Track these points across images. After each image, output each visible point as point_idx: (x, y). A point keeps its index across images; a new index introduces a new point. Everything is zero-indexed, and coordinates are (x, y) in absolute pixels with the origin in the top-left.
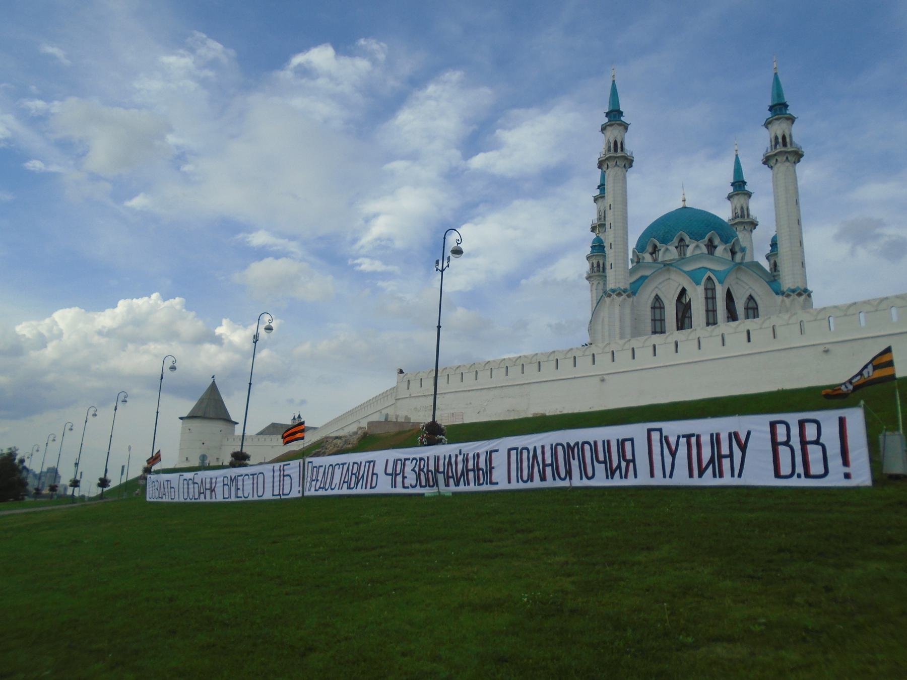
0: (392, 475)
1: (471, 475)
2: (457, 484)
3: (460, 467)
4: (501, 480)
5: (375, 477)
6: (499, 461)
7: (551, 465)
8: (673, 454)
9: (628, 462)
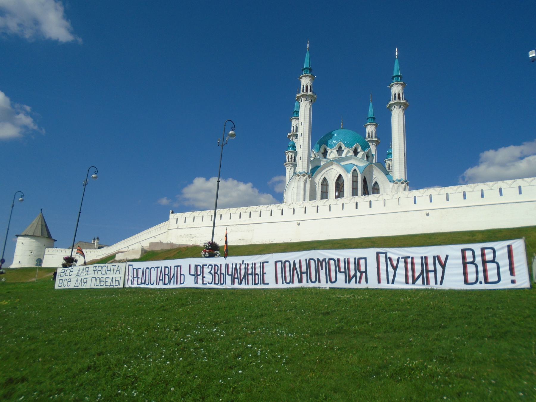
0: (194, 275)
1: (250, 277)
2: (240, 283)
3: (243, 272)
4: (271, 282)
5: (182, 277)
6: (269, 269)
7: (306, 273)
8: (395, 268)
9: (362, 273)
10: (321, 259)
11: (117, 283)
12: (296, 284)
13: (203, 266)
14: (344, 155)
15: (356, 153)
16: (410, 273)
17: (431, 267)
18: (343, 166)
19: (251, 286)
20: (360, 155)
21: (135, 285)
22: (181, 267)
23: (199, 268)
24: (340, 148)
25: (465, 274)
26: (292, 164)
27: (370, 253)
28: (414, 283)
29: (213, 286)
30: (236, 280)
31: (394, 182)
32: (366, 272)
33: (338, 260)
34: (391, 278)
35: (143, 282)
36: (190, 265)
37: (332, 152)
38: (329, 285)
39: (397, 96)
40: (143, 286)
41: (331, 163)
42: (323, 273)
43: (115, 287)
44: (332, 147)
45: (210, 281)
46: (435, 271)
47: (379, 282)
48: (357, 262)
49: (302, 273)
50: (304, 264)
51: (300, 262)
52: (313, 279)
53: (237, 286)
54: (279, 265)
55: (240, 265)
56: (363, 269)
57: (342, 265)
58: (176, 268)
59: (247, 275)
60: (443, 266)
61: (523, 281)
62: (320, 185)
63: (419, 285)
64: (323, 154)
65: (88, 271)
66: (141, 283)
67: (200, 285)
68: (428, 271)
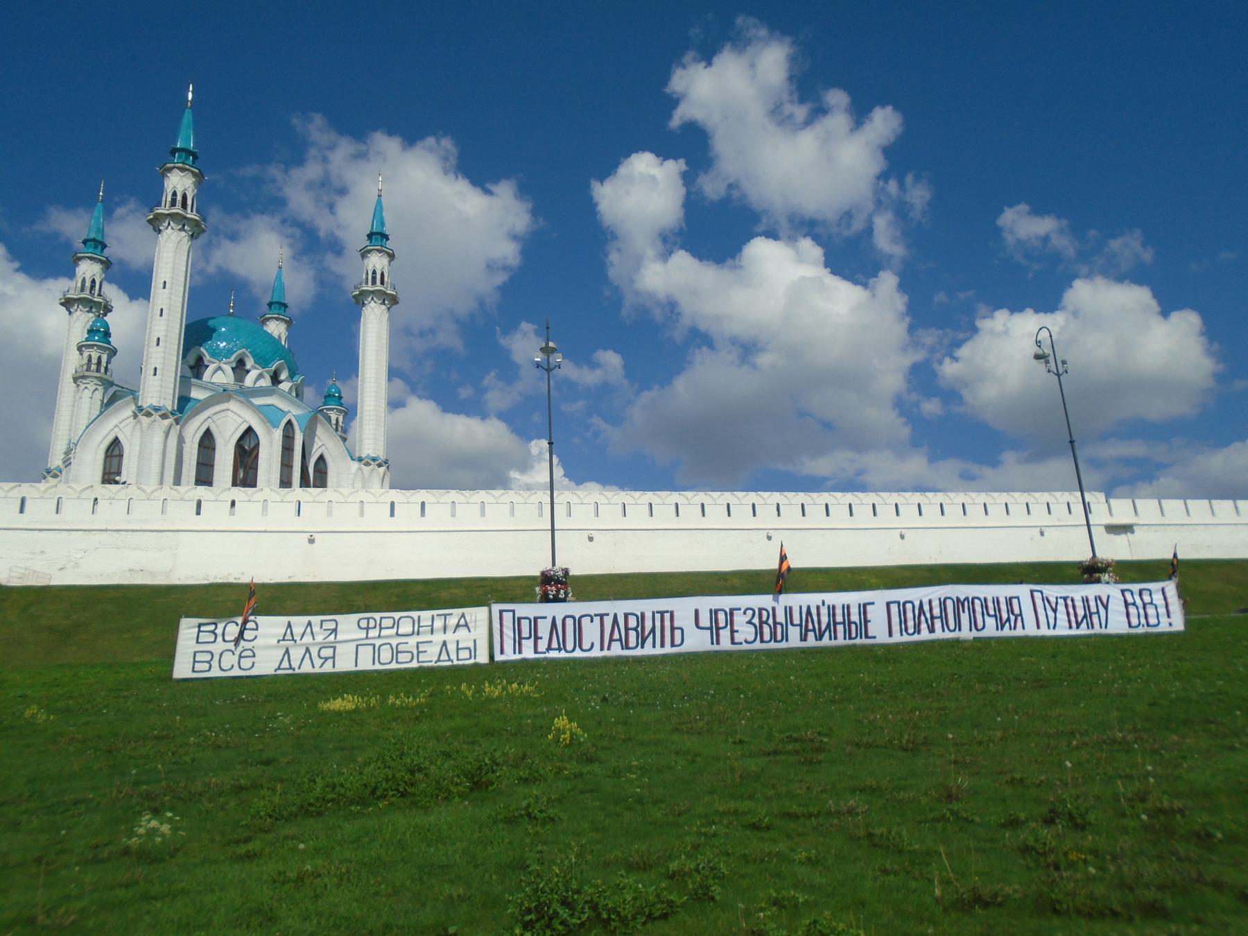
8: (1055, 611)
10: (962, 598)
11: (464, 654)
12: (925, 635)
13: (732, 611)
14: (249, 381)
15: (275, 379)
16: (1073, 618)
17: (1093, 609)
18: (258, 410)
19: (841, 641)
20: (285, 386)
21: (528, 653)
22: (672, 614)
23: (721, 616)
24: (241, 363)
25: (1128, 615)
26: (100, 379)
27: (1022, 591)
28: (1078, 627)
29: (758, 645)
30: (811, 635)
31: (360, 460)
32: (1021, 614)
33: (985, 600)
34: (1052, 621)
35: (554, 645)
36: (697, 612)
37: (219, 368)
38: (975, 634)
39: (378, 277)
40: (553, 654)
41: (223, 395)
42: (965, 618)
43: (456, 662)
44: (217, 354)
45: (751, 638)
46: (1098, 612)
47: (1038, 627)
48: (1009, 602)
49: (932, 618)
50: (936, 604)
51: (930, 602)
52: (952, 627)
53: (811, 641)
54: (894, 608)
55: (818, 608)
56: (1017, 611)
57: (990, 605)
58: (658, 616)
59: (832, 625)
60: (1106, 608)
61: (1176, 622)
62: (196, 446)
63: (1083, 630)
64: (191, 368)
65: (335, 631)
66: (549, 648)
67: (725, 644)
68: (1091, 614)
